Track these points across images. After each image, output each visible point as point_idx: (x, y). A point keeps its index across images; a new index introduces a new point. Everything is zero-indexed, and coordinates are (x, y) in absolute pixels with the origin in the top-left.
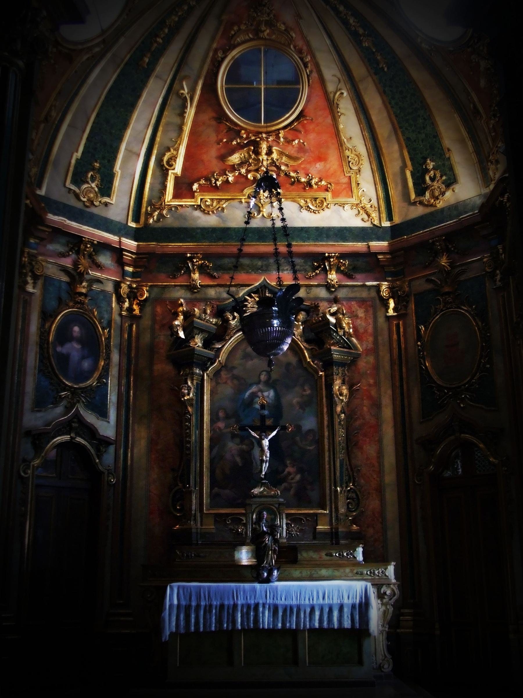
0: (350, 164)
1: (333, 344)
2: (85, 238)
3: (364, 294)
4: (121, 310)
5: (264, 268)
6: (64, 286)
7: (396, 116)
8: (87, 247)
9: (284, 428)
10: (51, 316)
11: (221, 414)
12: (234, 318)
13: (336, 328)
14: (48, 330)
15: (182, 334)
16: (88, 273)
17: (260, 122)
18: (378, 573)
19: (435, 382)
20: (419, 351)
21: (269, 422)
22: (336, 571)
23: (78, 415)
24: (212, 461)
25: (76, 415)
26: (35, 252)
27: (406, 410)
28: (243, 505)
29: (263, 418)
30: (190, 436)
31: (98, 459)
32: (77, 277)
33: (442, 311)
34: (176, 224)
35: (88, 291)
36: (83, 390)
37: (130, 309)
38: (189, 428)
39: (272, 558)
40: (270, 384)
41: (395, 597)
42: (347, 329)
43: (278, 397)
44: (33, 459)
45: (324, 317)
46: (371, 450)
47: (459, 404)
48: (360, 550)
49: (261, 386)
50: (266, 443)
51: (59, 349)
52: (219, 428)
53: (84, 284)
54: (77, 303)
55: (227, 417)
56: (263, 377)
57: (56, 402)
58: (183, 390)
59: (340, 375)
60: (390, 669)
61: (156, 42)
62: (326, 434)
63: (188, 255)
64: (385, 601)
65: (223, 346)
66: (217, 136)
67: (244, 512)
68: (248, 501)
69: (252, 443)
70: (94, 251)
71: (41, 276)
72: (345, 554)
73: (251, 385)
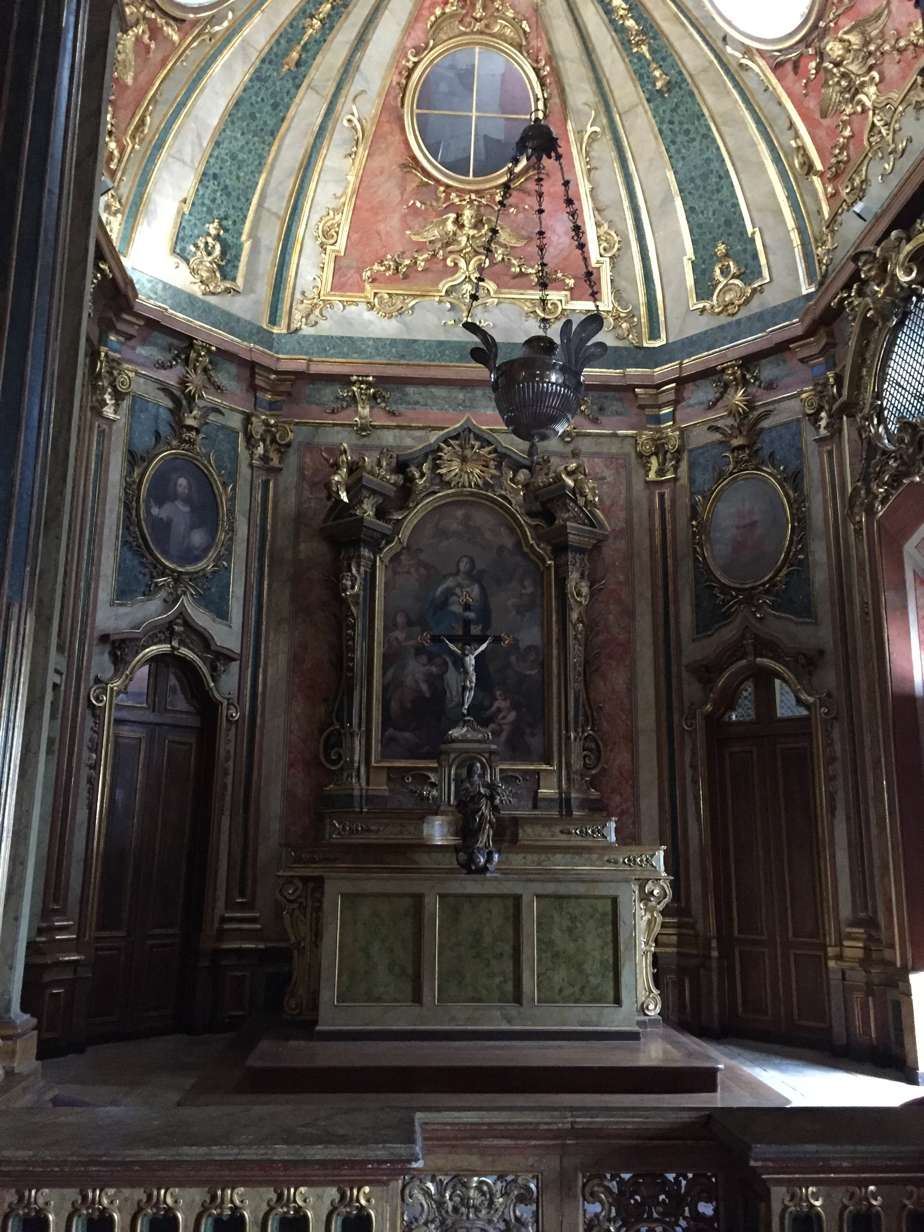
0: (602, 247)
1: (568, 519)
2: (197, 340)
3: (614, 448)
4: (252, 458)
5: (468, 403)
6: (164, 415)
7: (675, 173)
8: (200, 355)
9: (497, 639)
10: (143, 459)
11: (400, 619)
12: (422, 475)
13: (575, 495)
14: (137, 480)
15: (344, 497)
16: (201, 397)
17: (468, 175)
18: (641, 861)
19: (718, 581)
20: (694, 534)
21: (475, 630)
22: (577, 857)
23: (182, 615)
24: (385, 689)
25: (181, 613)
26: (118, 355)
27: (672, 621)
28: (435, 755)
29: (467, 623)
30: (353, 650)
31: (214, 682)
32: (184, 402)
33: (731, 474)
34: (337, 332)
35: (202, 425)
36: (193, 576)
37: (265, 458)
38: (352, 639)
39: (485, 838)
40: (474, 576)
41: (666, 899)
42: (590, 497)
43: (484, 594)
44: (111, 679)
45: (558, 478)
46: (618, 679)
47: (754, 613)
48: (612, 825)
49: (460, 579)
50: (471, 661)
51: (155, 511)
52: (397, 639)
53: (195, 412)
54: (185, 441)
55: (410, 623)
56: (464, 566)
57: (149, 592)
58: (344, 581)
59: (578, 565)
60: (658, 1010)
61: (311, 26)
62: (555, 652)
63: (355, 378)
64: (650, 904)
65: (405, 518)
66: (402, 195)
67: (436, 765)
68: (443, 747)
69: (446, 664)
70: (211, 362)
71: (128, 393)
72: (590, 831)
73: (445, 577)
